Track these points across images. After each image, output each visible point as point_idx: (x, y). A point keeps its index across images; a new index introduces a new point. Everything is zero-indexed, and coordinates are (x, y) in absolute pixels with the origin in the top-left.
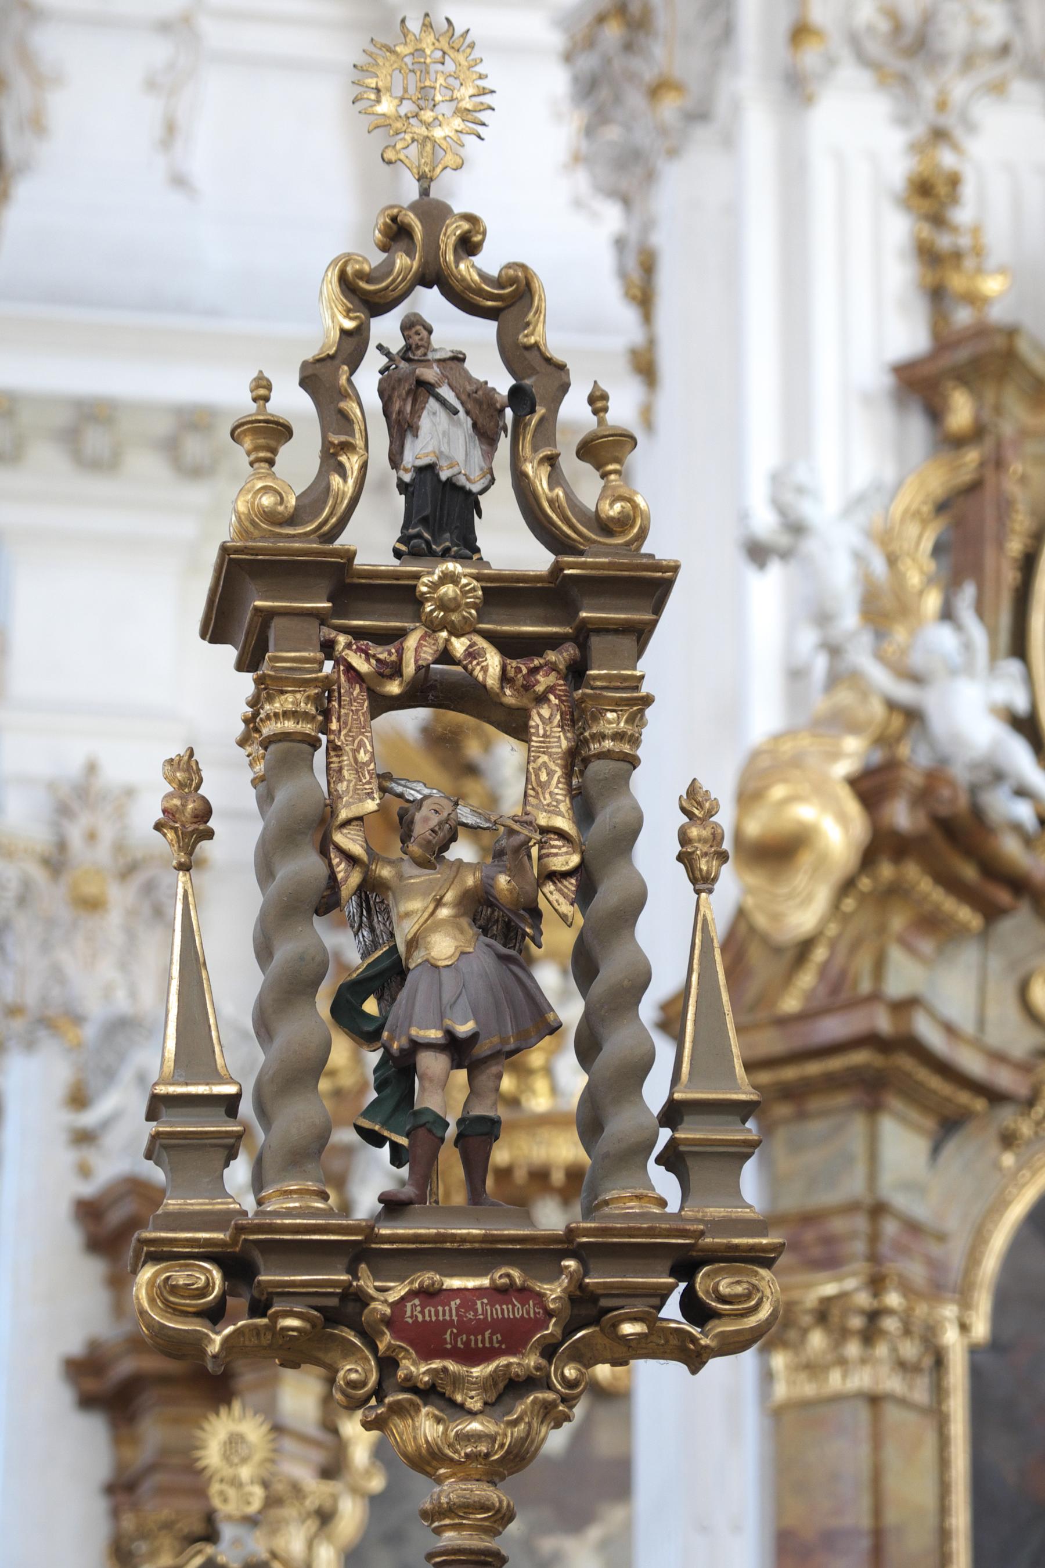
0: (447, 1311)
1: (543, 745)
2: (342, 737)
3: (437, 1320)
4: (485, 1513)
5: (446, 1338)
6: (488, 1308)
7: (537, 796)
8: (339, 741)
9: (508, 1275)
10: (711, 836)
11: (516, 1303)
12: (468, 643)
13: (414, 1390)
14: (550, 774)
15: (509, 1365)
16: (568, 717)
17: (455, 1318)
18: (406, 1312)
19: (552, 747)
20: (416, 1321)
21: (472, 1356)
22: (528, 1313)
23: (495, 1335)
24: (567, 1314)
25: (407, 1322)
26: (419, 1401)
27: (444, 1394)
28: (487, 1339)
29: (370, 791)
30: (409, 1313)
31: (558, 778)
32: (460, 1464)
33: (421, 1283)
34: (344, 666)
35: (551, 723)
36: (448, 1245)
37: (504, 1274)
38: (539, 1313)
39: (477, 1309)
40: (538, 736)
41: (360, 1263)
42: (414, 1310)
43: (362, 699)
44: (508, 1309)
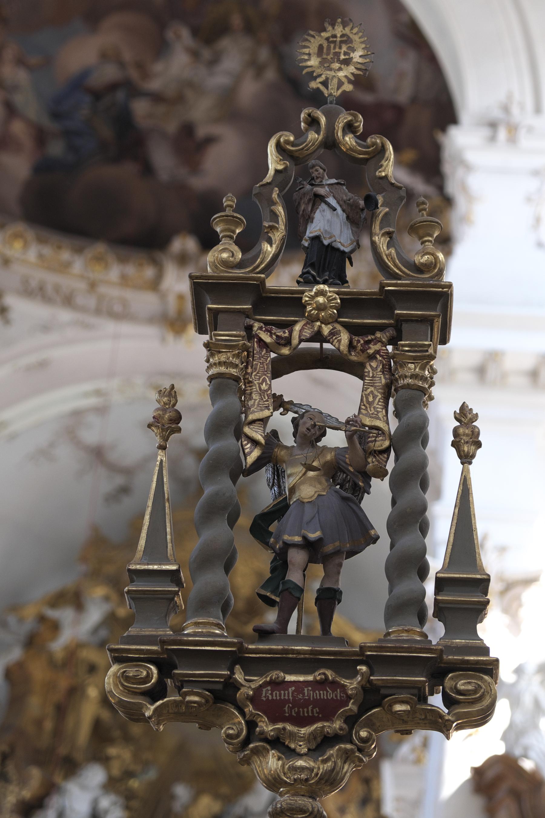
0: (287, 694)
1: (371, 382)
2: (253, 376)
3: (280, 699)
4: (303, 814)
5: (285, 710)
6: (311, 692)
7: (366, 409)
8: (251, 378)
9: (324, 674)
10: (471, 433)
11: (329, 690)
12: (332, 328)
13: (266, 740)
14: (375, 397)
15: (324, 727)
16: (387, 367)
18: (262, 693)
19: (377, 383)
21: (301, 722)
22: (336, 696)
23: (314, 709)
24: (361, 698)
25: (262, 699)
26: (268, 747)
27: (284, 743)
29: (267, 405)
30: (264, 694)
31: (379, 399)
32: (291, 785)
33: (271, 678)
34: (257, 339)
35: (377, 370)
36: (290, 656)
37: (321, 673)
38: (343, 697)
39: (305, 693)
40: (369, 377)
41: (236, 664)
42: (267, 694)
43: (267, 357)
44: (324, 694)
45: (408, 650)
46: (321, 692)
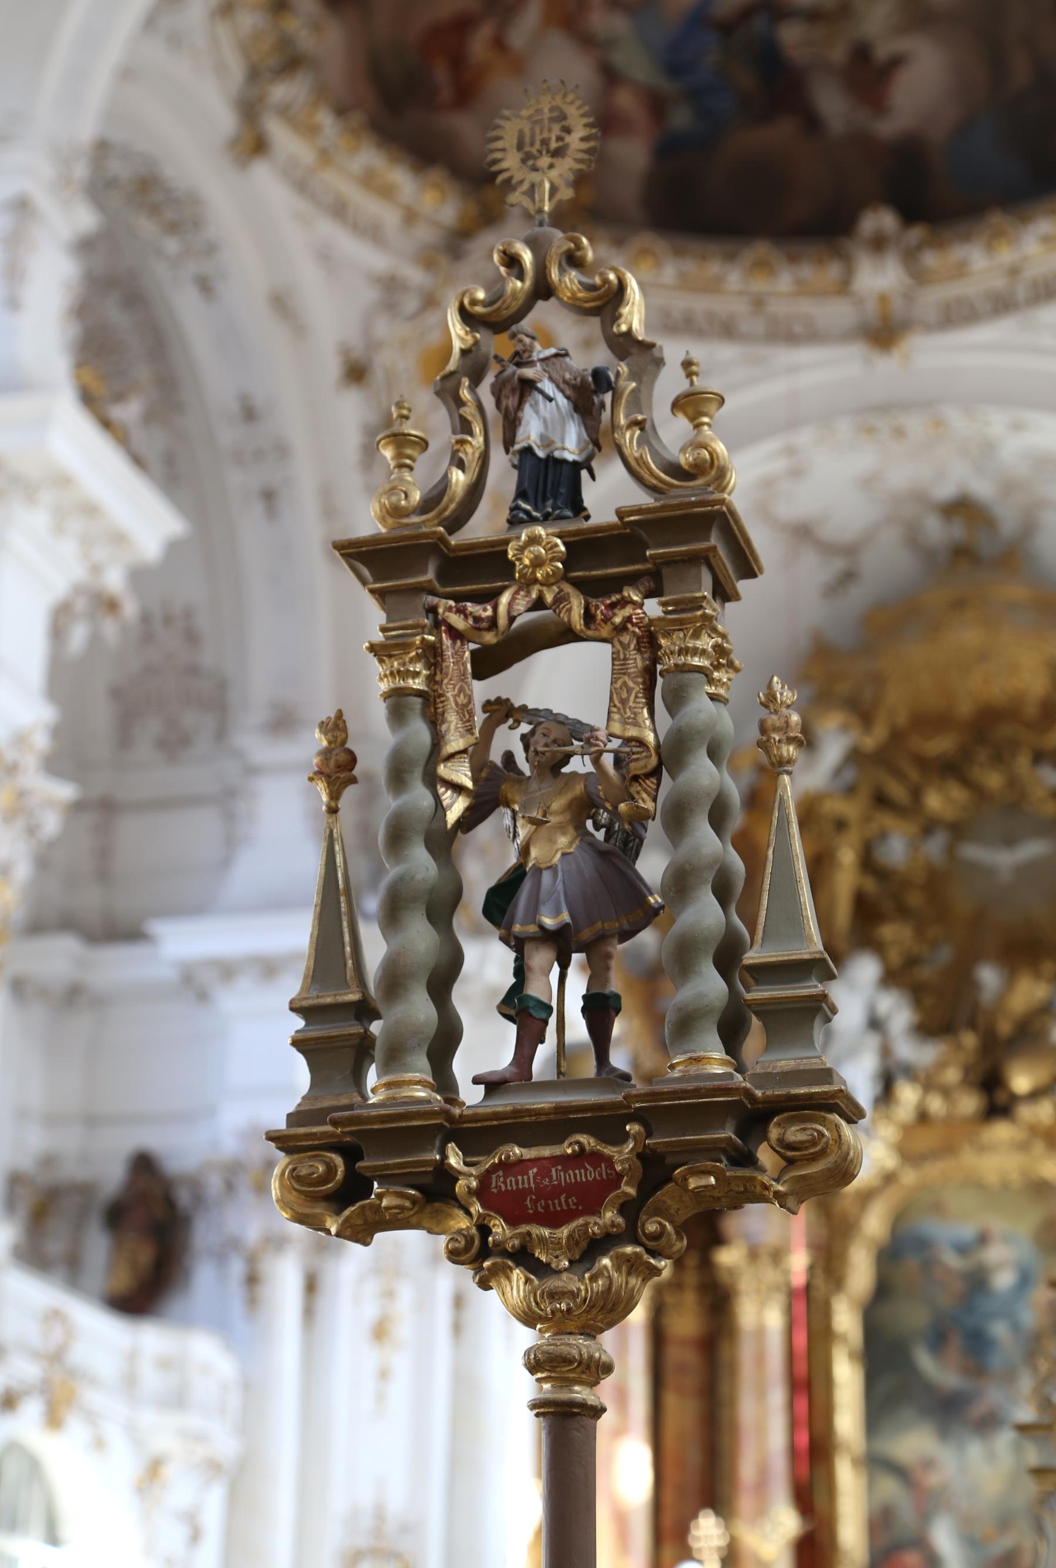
0: (526, 1180)
1: (623, 667)
2: (444, 686)
3: (517, 1188)
4: (569, 1366)
5: (527, 1205)
7: (619, 712)
8: (441, 689)
9: (578, 1142)
11: (588, 1167)
12: (557, 590)
13: (505, 1254)
14: (629, 691)
15: (586, 1225)
16: (645, 640)
17: (532, 1185)
18: (492, 1183)
19: (630, 668)
20: (500, 1191)
21: (554, 1220)
22: (600, 1175)
24: (639, 1172)
25: (493, 1192)
26: (510, 1263)
27: (534, 1255)
28: (562, 1203)
29: (470, 727)
30: (494, 1184)
31: (636, 694)
32: (548, 1320)
34: (445, 626)
35: (629, 647)
36: (527, 1119)
37: (573, 1142)
38: (611, 1174)
39: (552, 1176)
40: (619, 660)
41: (449, 1142)
42: (500, 1183)
43: (462, 652)
45: (696, 1093)
46: (577, 1171)
